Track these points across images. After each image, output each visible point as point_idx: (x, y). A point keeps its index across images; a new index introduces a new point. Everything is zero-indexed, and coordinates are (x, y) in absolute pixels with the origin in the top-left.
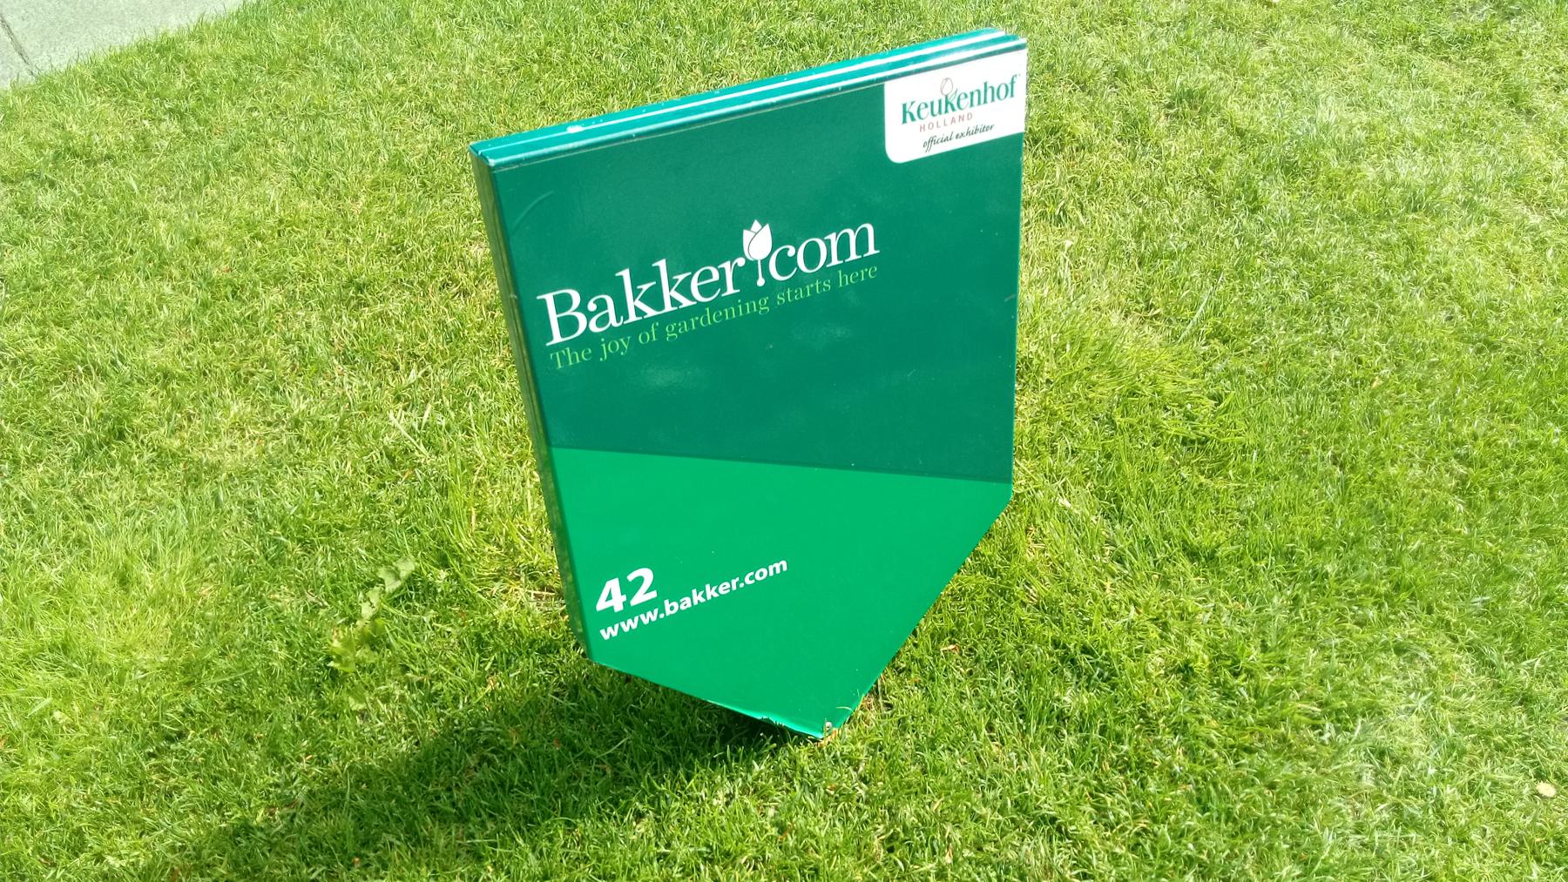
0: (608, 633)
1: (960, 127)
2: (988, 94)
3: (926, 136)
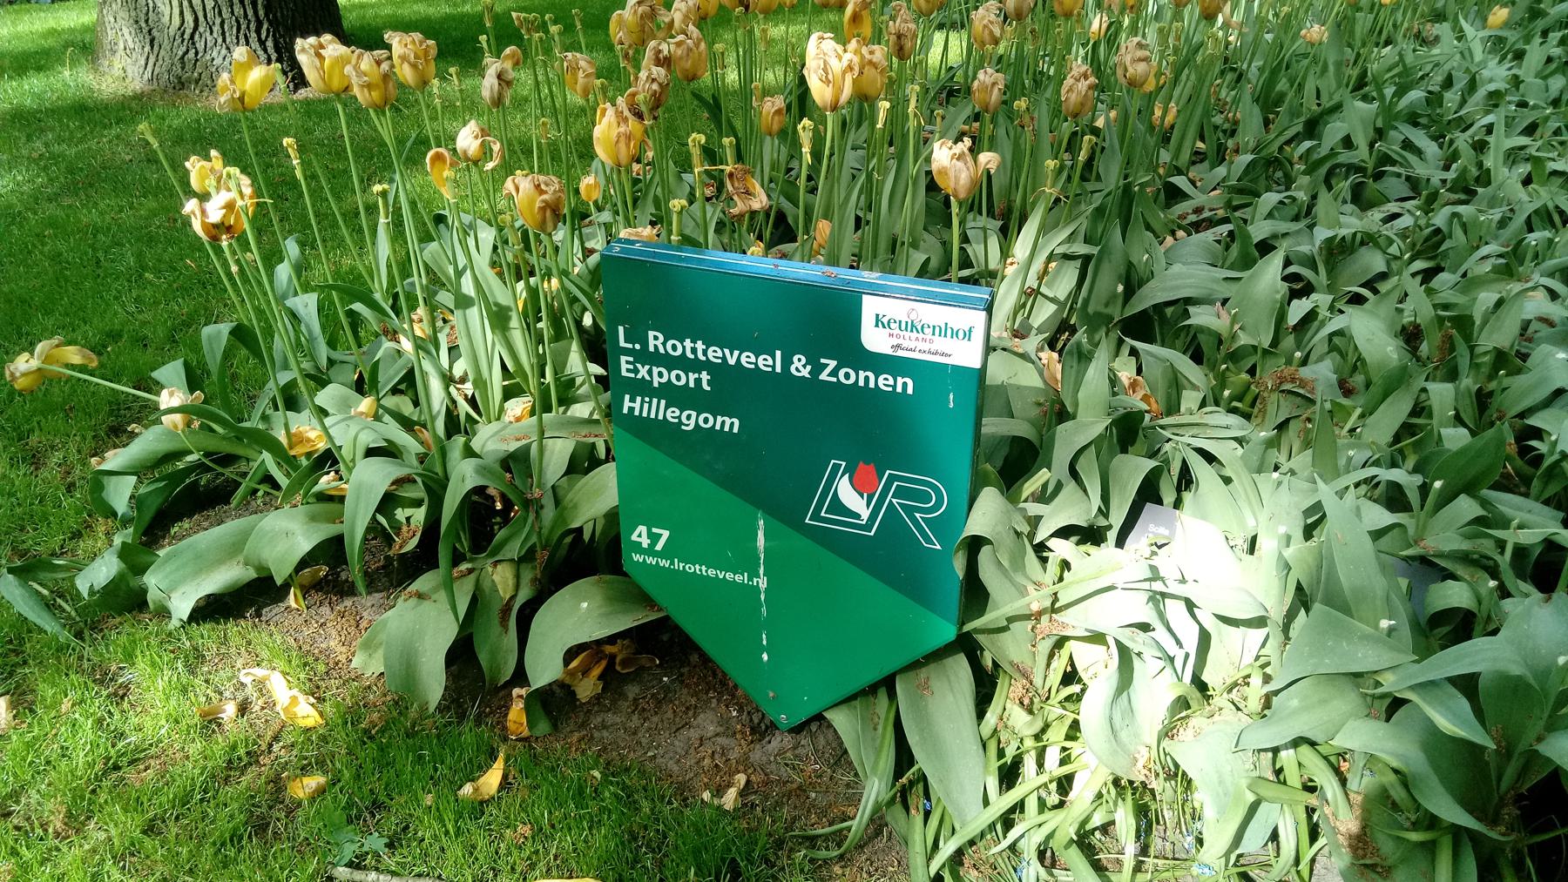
0: (637, 558)
1: (925, 346)
2: (944, 331)
3: (895, 342)
